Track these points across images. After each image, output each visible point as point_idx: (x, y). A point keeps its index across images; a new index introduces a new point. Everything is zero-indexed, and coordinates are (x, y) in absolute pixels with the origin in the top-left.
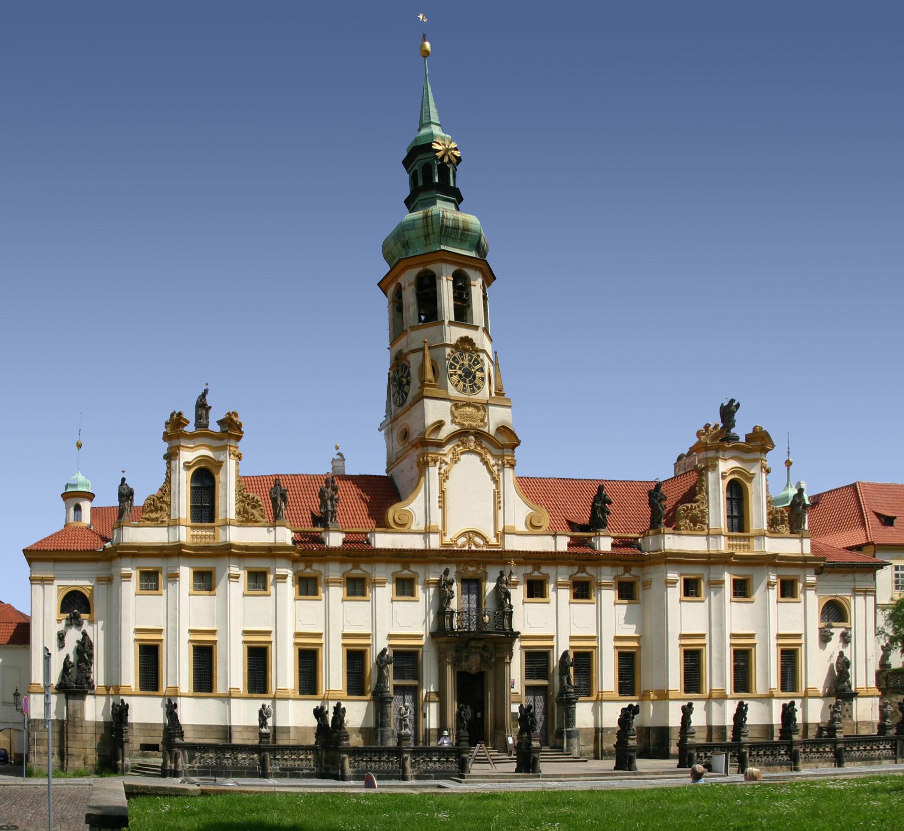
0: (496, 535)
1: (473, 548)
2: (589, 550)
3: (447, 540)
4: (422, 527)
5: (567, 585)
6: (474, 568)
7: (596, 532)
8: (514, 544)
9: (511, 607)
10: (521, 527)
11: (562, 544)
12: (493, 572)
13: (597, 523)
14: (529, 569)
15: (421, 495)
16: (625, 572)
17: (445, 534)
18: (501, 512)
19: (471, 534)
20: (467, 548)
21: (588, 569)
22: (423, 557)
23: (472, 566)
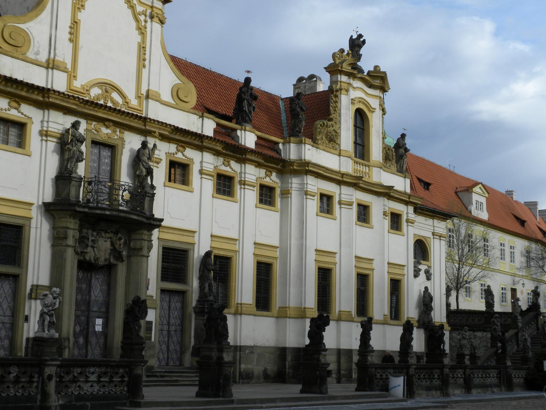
0: (138, 97)
1: (109, 104)
2: (234, 143)
3: (77, 84)
4: (43, 57)
5: (212, 176)
6: (109, 131)
7: (242, 125)
8: (156, 112)
9: (153, 187)
10: (167, 97)
11: (208, 127)
12: (132, 142)
13: (241, 116)
14: (172, 148)
15: (45, 15)
16: (266, 175)
17: (75, 77)
18: (145, 72)
19: (108, 87)
20: (101, 102)
21: (233, 163)
22: (42, 98)
23: (107, 127)
